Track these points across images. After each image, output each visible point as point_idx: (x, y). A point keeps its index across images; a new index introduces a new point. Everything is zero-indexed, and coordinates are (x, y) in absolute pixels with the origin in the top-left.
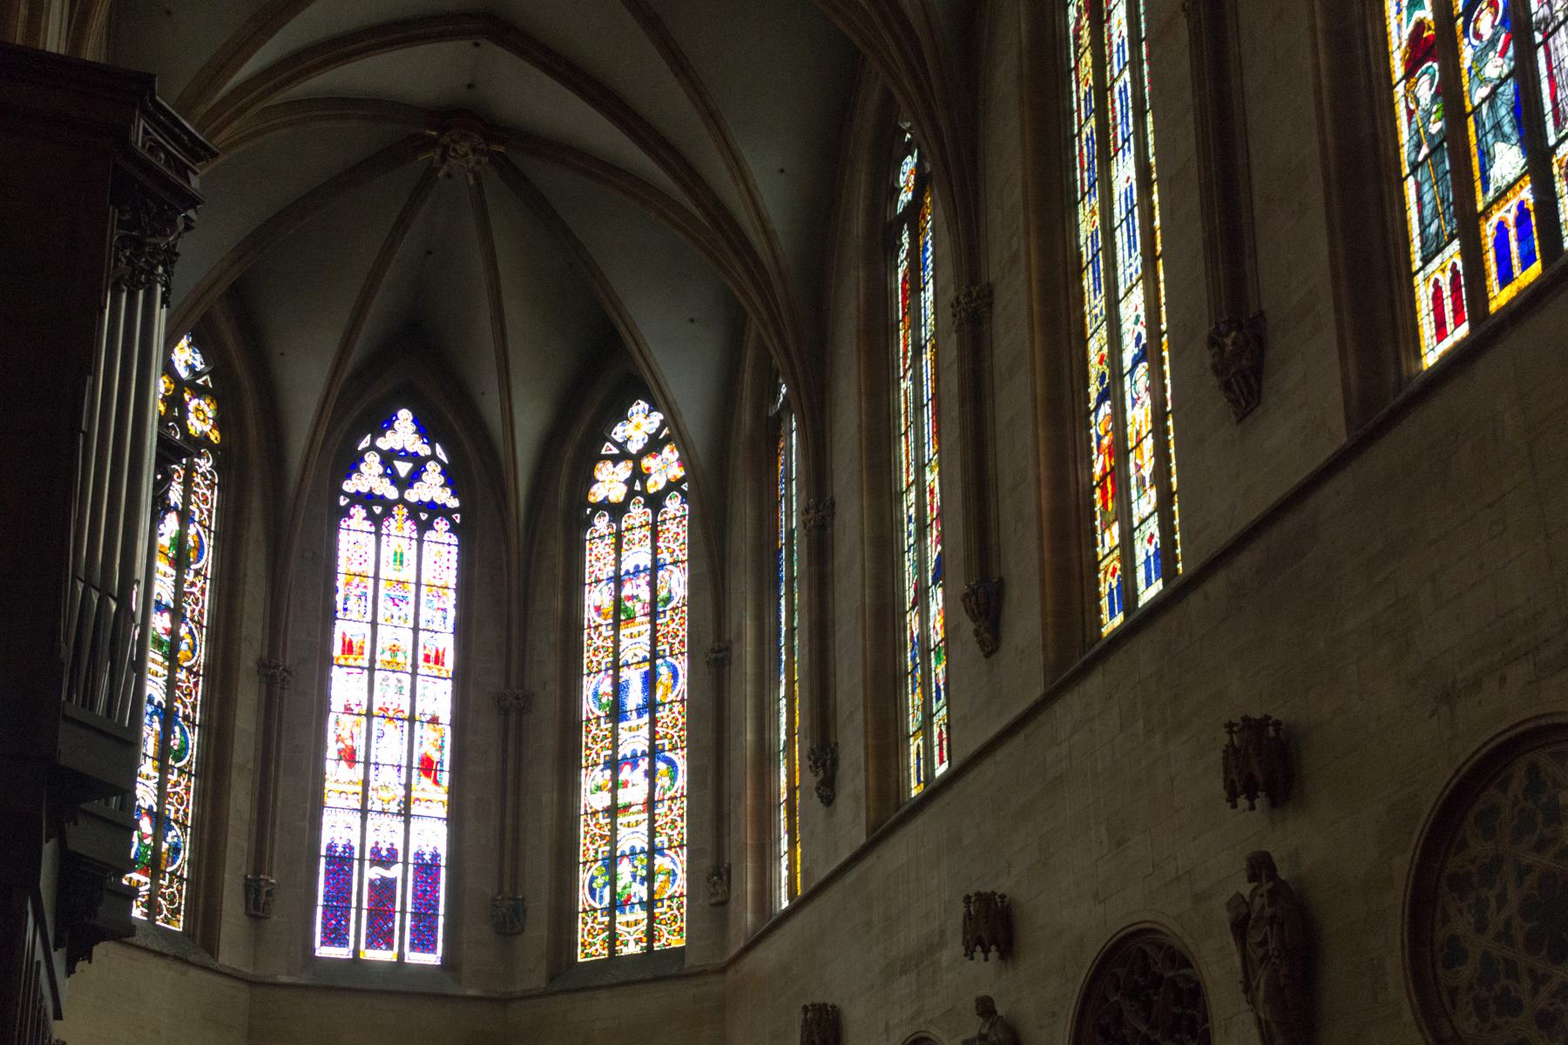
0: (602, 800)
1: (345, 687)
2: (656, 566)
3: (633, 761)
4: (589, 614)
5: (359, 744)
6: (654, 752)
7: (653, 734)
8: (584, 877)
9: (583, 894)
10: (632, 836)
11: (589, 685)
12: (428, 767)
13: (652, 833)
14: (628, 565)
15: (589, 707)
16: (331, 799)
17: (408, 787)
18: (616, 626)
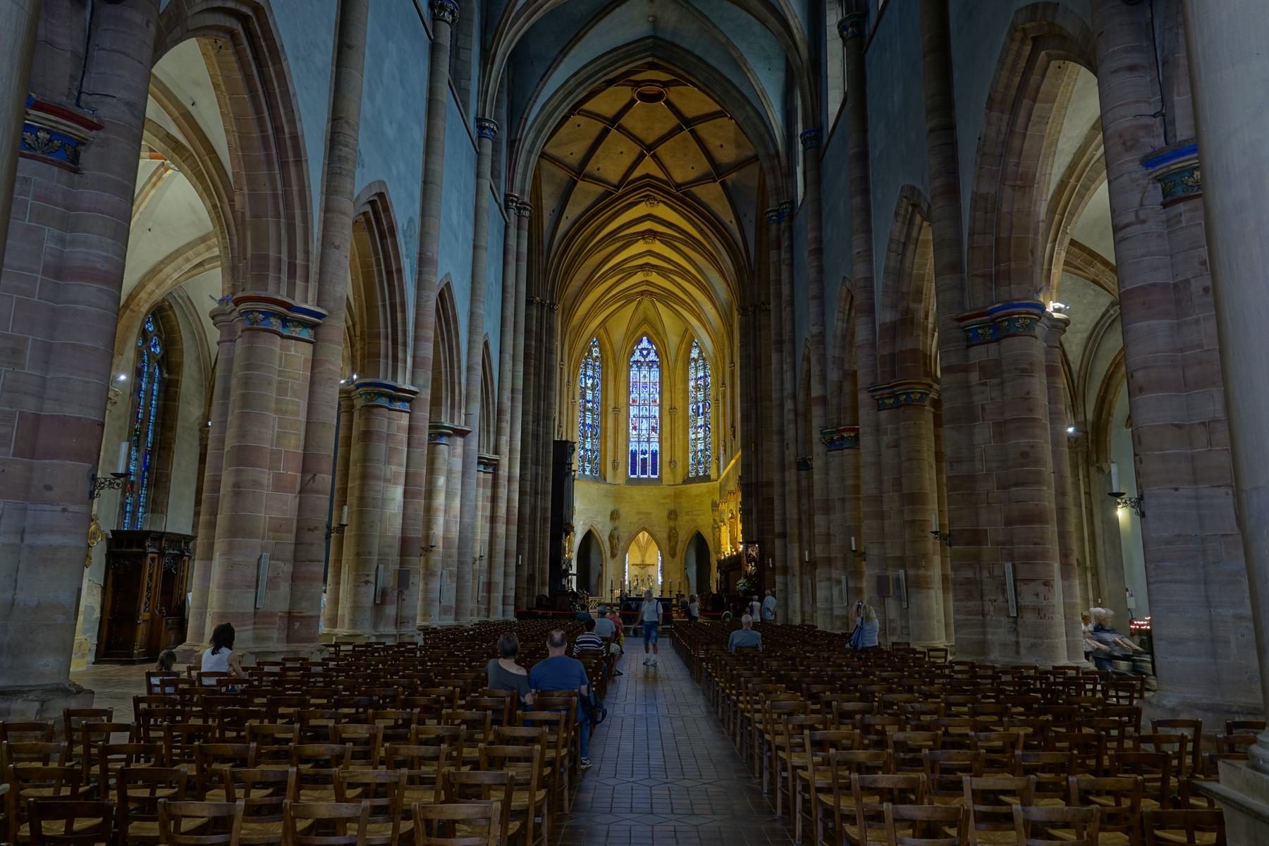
0: (693, 437)
1: (633, 411)
2: (705, 376)
3: (701, 427)
4: (691, 388)
5: (637, 425)
6: (706, 425)
7: (705, 421)
8: (691, 455)
9: (691, 460)
10: (700, 446)
11: (691, 406)
12: (654, 429)
13: (705, 446)
14: (699, 376)
15: (691, 413)
16: (632, 440)
17: (649, 434)
18: (696, 392)
